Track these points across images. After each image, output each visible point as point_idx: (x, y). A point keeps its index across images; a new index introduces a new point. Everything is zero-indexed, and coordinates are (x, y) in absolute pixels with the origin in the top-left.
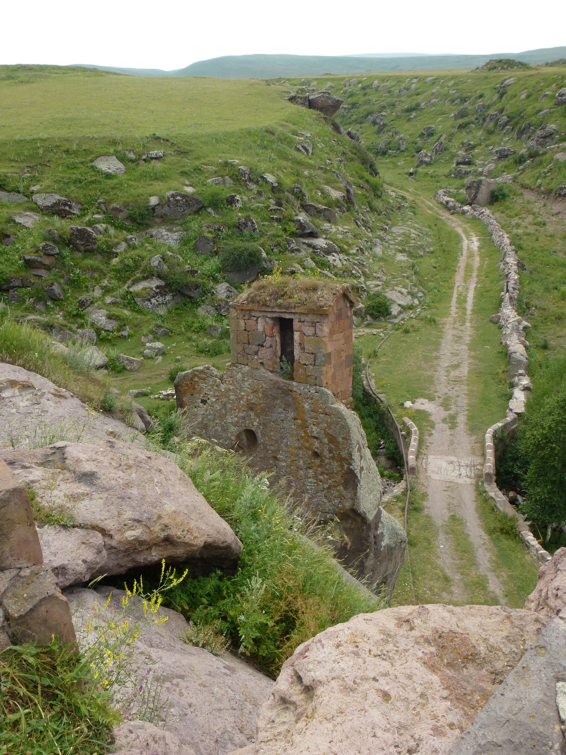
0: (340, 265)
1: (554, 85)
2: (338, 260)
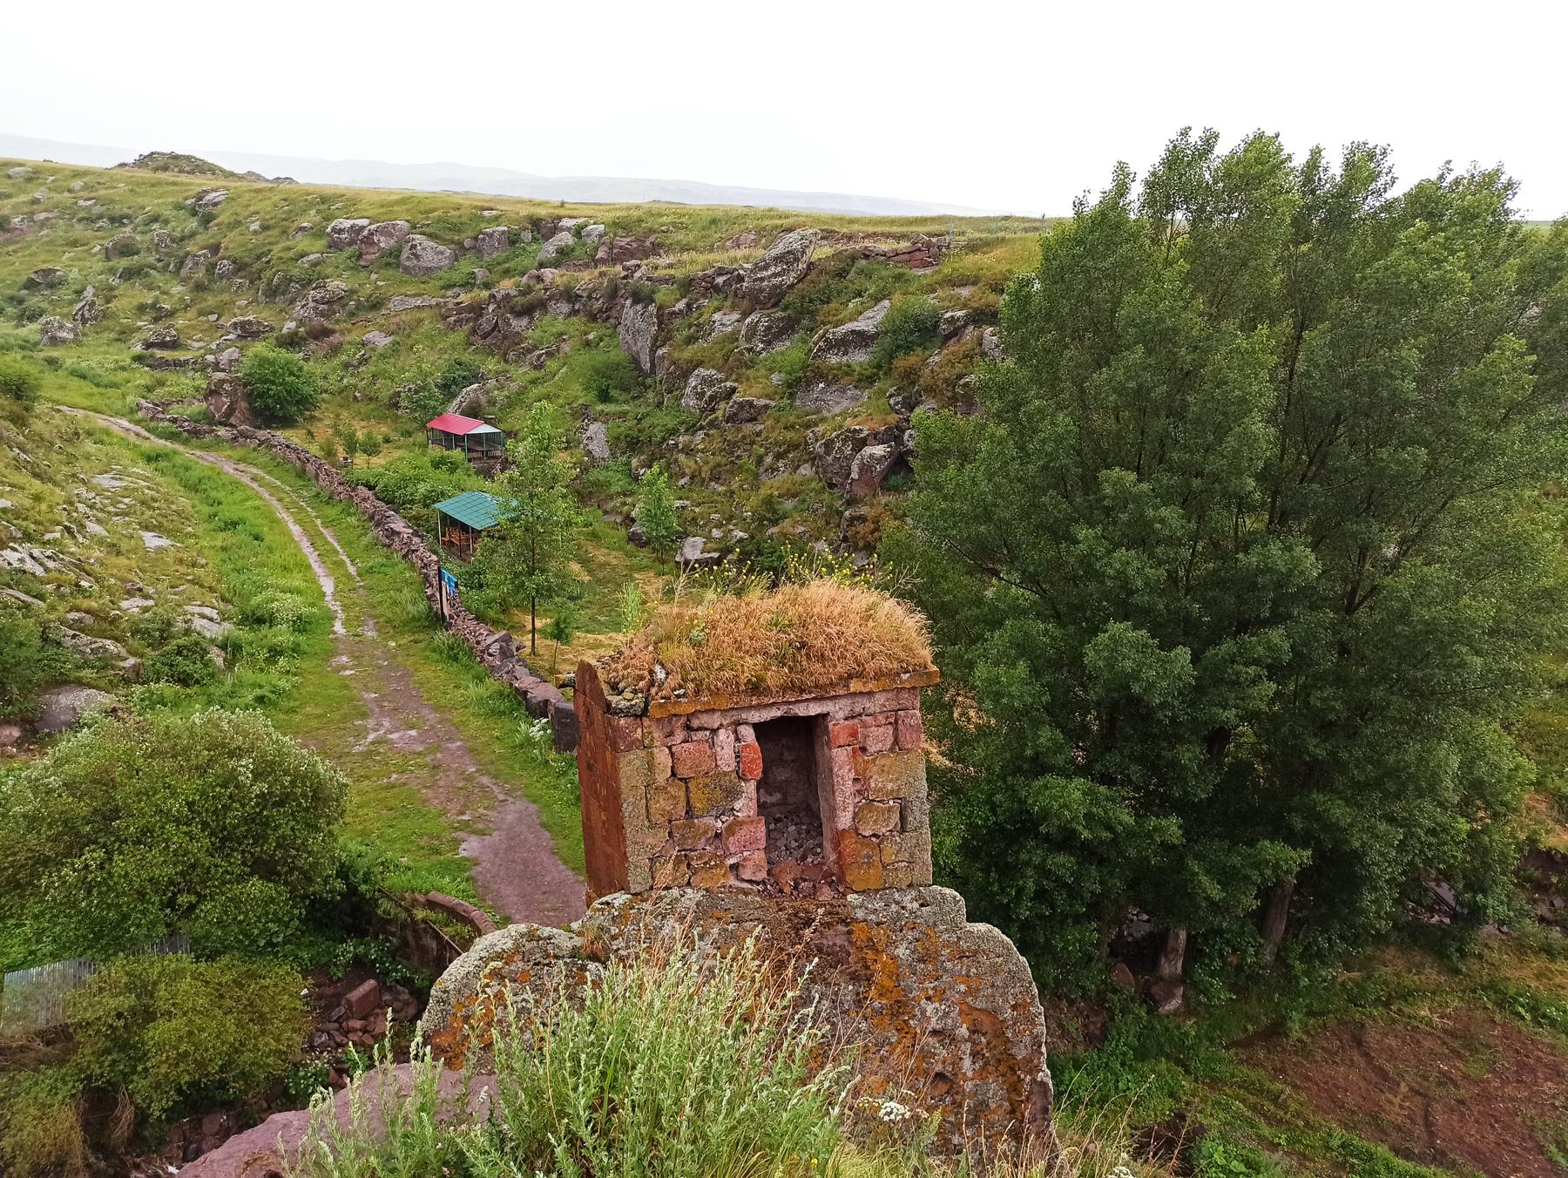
0: (39, 571)
1: (313, 212)
2: (28, 559)
